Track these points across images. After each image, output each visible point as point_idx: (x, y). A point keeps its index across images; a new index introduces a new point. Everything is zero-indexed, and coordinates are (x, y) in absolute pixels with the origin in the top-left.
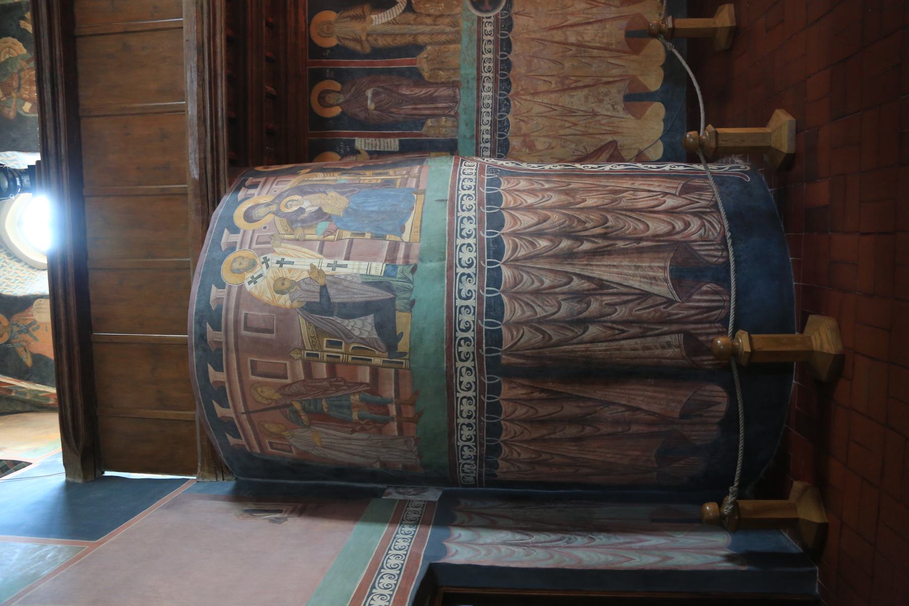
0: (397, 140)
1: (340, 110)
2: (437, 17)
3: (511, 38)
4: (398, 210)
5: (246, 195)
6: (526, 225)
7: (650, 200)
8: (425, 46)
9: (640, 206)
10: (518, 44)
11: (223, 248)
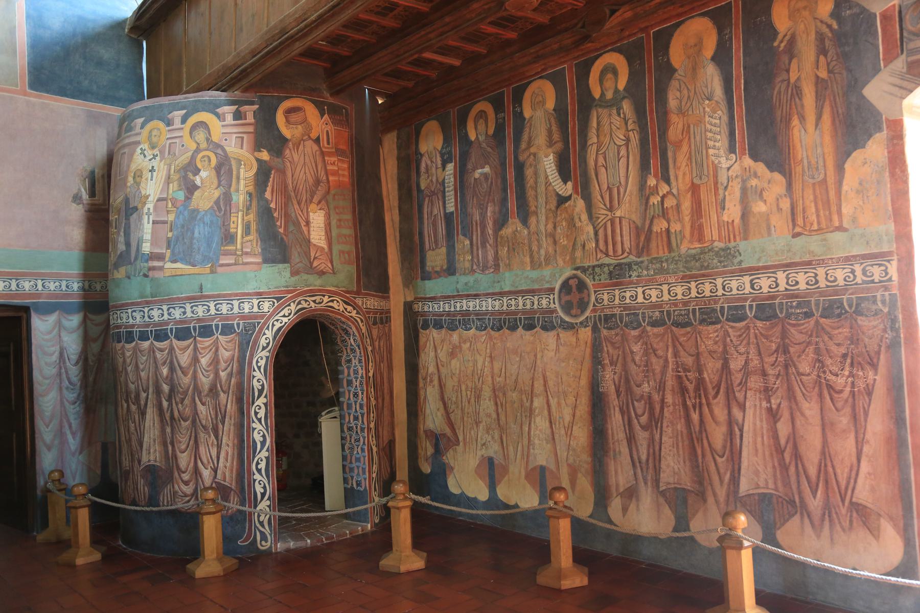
0: (452, 209)
1: (473, 140)
2: (552, 236)
3: (535, 330)
4: (194, 254)
5: (224, 114)
6: (179, 358)
7: (207, 458)
8: (527, 226)
9: (200, 448)
10: (532, 338)
11: (170, 116)
